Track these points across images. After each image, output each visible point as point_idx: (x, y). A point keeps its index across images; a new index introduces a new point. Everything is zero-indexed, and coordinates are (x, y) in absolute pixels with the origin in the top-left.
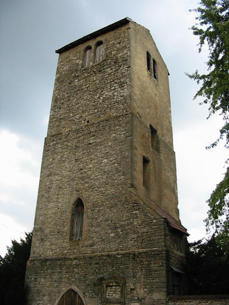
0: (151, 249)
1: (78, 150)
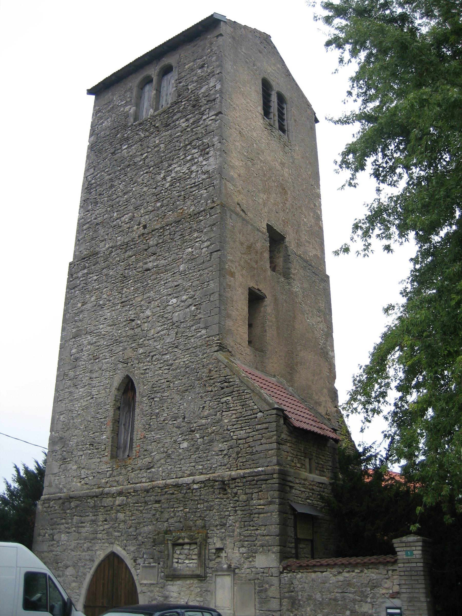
0: (251, 470)
1: (127, 283)
